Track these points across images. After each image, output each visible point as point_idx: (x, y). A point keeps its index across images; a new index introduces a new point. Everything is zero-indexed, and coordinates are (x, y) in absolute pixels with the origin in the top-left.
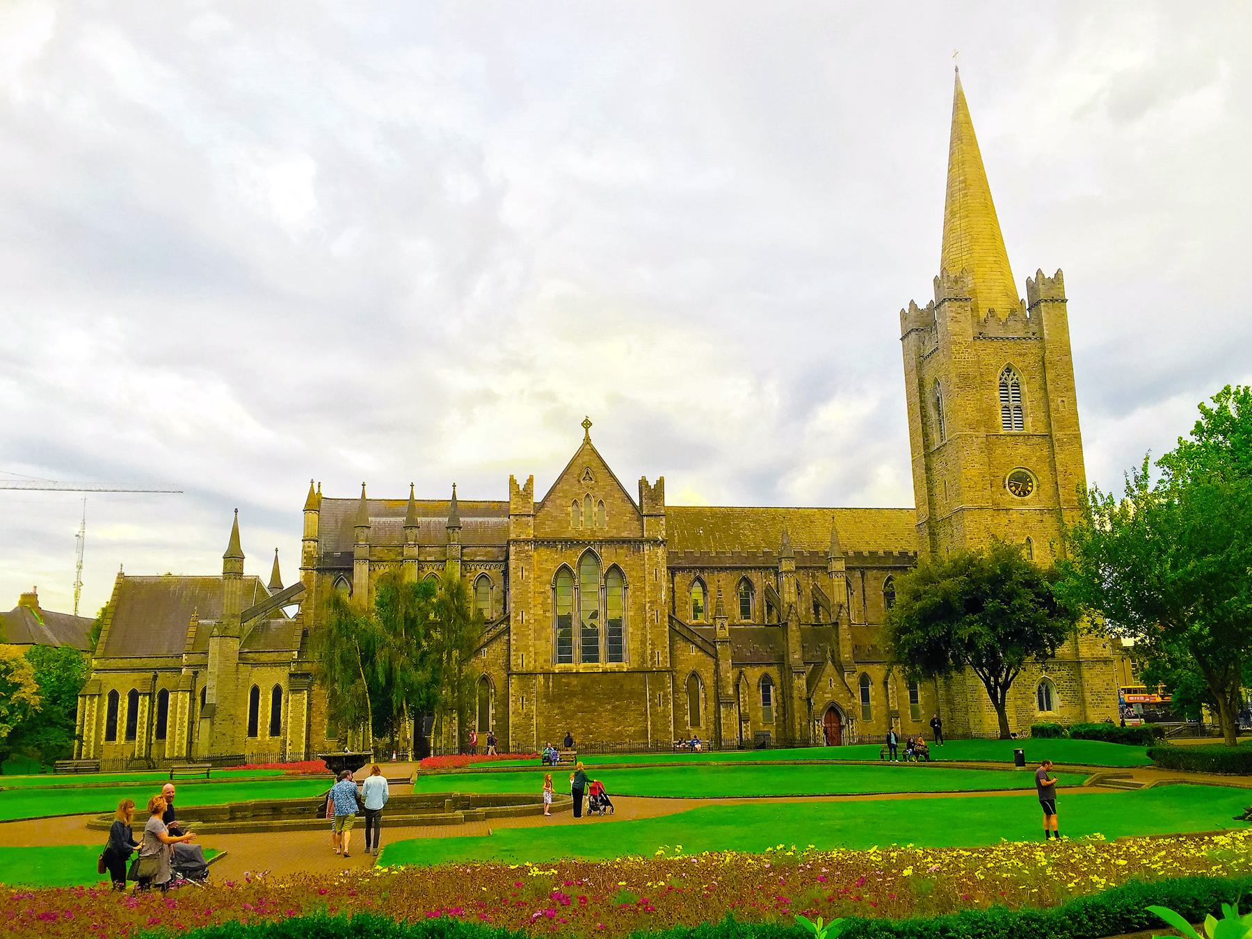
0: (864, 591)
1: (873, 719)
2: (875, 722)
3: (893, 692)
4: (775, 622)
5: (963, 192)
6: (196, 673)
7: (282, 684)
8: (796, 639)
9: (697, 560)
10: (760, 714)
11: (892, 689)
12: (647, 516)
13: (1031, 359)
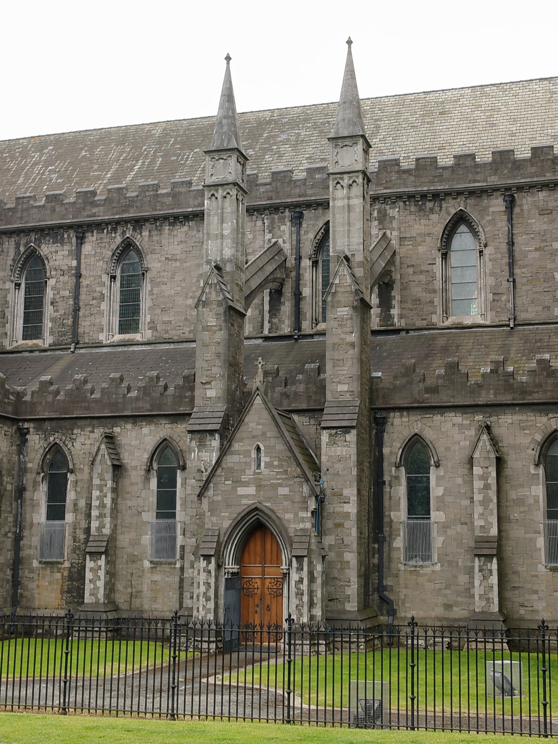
0: (511, 243)
1: (435, 558)
2: (438, 567)
3: (487, 487)
4: (286, 329)
8: (213, 349)
9: (132, 202)
10: (147, 539)
11: (484, 477)
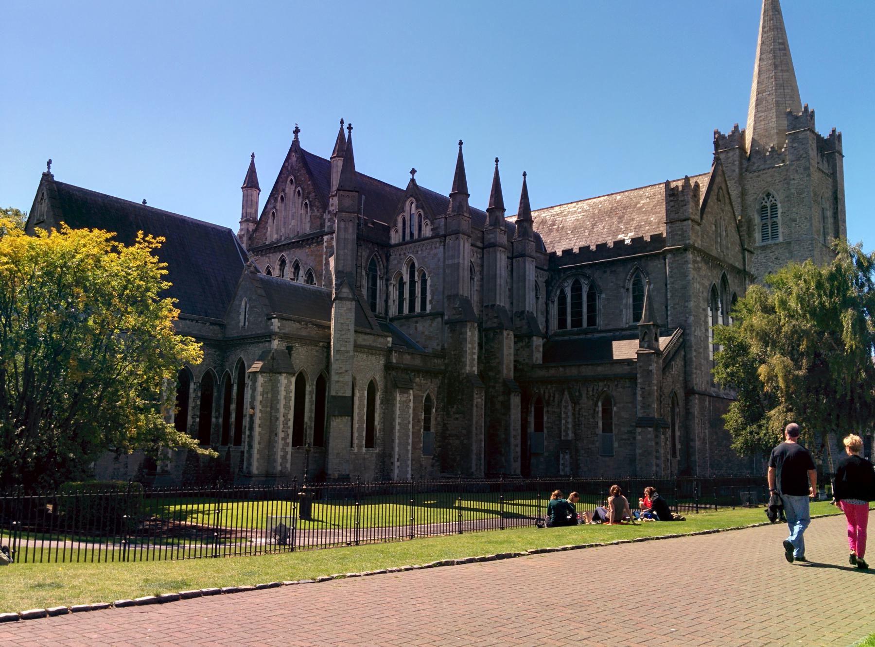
5: (782, 52)
6: (289, 349)
7: (377, 378)
12: (748, 251)
13: (830, 193)
